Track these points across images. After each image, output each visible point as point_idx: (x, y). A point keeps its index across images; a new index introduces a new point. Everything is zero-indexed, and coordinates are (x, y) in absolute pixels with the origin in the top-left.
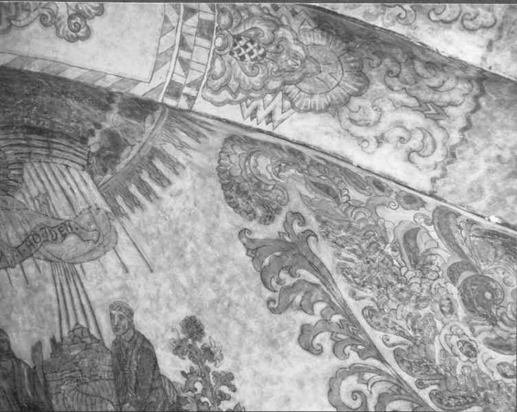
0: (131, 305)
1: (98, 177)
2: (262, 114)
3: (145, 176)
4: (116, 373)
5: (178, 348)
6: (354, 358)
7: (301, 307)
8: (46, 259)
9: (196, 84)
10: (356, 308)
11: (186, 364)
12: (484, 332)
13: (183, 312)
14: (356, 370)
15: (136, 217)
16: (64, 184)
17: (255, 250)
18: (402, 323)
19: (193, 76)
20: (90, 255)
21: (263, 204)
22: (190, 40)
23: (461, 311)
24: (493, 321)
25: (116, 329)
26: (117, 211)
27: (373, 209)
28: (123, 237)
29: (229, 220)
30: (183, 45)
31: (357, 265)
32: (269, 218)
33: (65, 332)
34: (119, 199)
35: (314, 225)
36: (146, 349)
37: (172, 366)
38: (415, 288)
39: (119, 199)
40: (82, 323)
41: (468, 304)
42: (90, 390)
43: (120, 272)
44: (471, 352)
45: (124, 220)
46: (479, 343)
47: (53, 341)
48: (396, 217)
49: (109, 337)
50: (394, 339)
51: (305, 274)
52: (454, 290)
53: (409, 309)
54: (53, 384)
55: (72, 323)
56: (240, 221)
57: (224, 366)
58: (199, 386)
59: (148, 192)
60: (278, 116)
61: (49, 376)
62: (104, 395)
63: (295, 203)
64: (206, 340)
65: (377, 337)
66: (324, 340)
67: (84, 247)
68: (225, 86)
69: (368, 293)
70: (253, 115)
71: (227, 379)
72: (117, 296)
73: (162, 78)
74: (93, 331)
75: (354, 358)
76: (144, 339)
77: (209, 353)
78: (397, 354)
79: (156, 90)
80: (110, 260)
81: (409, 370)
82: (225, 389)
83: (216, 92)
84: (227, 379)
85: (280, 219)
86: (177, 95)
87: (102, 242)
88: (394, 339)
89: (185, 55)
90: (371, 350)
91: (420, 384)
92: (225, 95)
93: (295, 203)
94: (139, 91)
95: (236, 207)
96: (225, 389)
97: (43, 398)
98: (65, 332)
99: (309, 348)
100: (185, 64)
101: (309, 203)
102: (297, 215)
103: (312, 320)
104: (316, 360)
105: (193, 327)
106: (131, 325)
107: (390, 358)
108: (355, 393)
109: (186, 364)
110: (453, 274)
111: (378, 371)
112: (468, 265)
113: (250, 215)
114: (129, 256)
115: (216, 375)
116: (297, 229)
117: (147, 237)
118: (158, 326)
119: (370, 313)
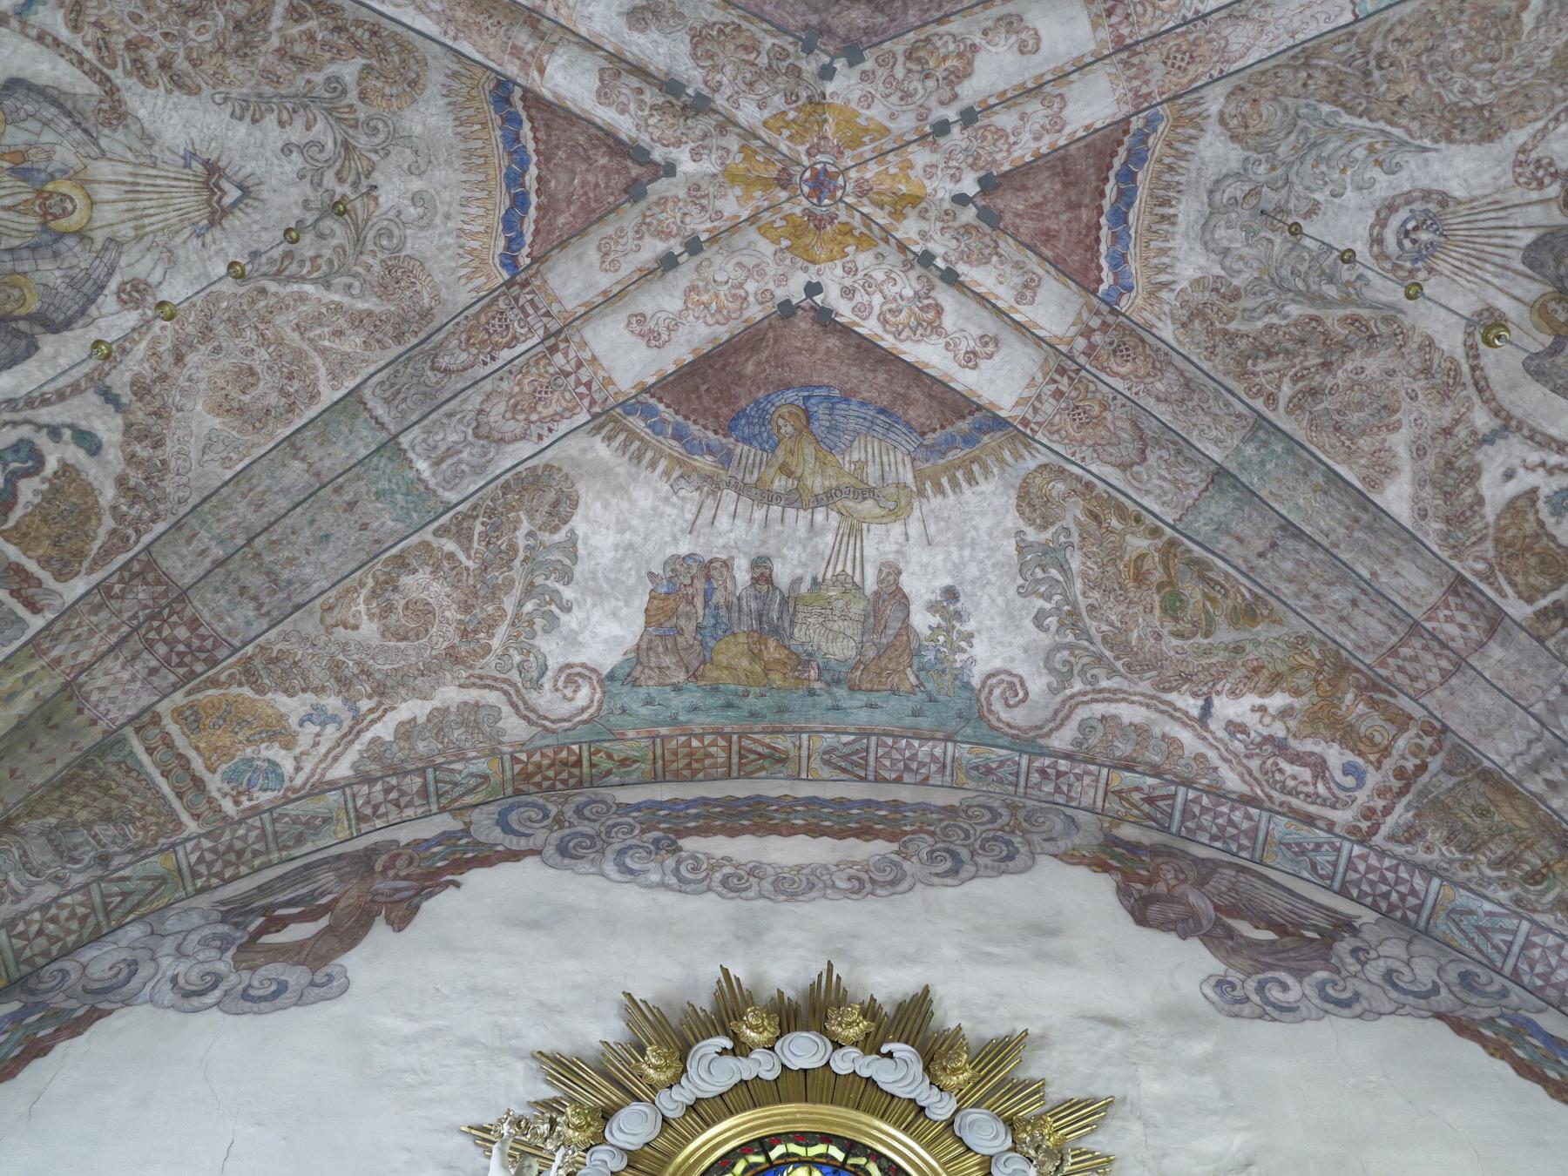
0: (901, 566)
1: (918, 463)
2: (1078, 456)
3: (959, 474)
4: (866, 617)
5: (932, 607)
6: (1070, 638)
7: (1042, 596)
8: (840, 512)
9: (1039, 424)
10: (1083, 603)
11: (935, 620)
12: (1170, 625)
13: (947, 581)
14: (1071, 647)
15: (936, 501)
16: (885, 459)
17: (1021, 549)
18: (1113, 617)
19: (1039, 419)
20: (879, 520)
21: (1043, 517)
22: (1044, 397)
23: (1157, 612)
24: (1176, 620)
25: (880, 582)
26: (921, 493)
27: (1123, 535)
28: (916, 513)
29: (1012, 520)
30: (1039, 397)
31: (1095, 572)
32: (1044, 527)
33: (829, 575)
34: (928, 485)
35: (1075, 539)
36: (904, 601)
37: (922, 620)
38: (1131, 595)
39: (928, 485)
40: (849, 571)
41: (1164, 610)
42: (836, 627)
43: (902, 540)
44: (1159, 637)
45: (924, 500)
46: (1165, 632)
47: (814, 579)
48: (1138, 543)
49: (870, 586)
50: (1104, 627)
51: (1054, 572)
52: (1157, 598)
53: (1122, 608)
54: (800, 615)
55: (839, 569)
56: (1021, 524)
57: (970, 626)
58: (941, 639)
59: (955, 485)
60: (1088, 460)
61: (800, 608)
62: (849, 632)
63: (1069, 521)
64: (959, 605)
65: (1092, 626)
66: (1052, 621)
67: (877, 511)
68: (1058, 431)
69: (1096, 594)
70: (1073, 454)
71: (969, 637)
72: (891, 557)
73: (1019, 412)
74: (857, 579)
75: (1070, 638)
76: (905, 596)
77: (958, 615)
78: (1104, 638)
79: (1015, 418)
80: (897, 529)
81: (1111, 649)
82: (963, 644)
83: (1052, 433)
84: (969, 637)
85: (1052, 530)
86: (1026, 426)
87: (897, 512)
88: (1104, 627)
89: (1038, 405)
90: (1084, 633)
91: (1118, 658)
92: (1056, 437)
93: (1069, 521)
94: (1003, 414)
95: (1022, 514)
96: (963, 644)
97: (786, 624)
98: (829, 575)
99: (1039, 626)
100: (1036, 410)
101: (1078, 523)
102: (1067, 530)
103: (1048, 606)
104: (1043, 635)
105: (951, 594)
106: (896, 581)
107: (1098, 638)
108: (1065, 663)
109: (935, 620)
110: (1160, 586)
111: (1086, 649)
112: (1170, 583)
113: (1031, 521)
114: (914, 529)
115: (959, 632)
116: (1062, 539)
117: (937, 518)
118: (920, 586)
119: (1092, 608)
